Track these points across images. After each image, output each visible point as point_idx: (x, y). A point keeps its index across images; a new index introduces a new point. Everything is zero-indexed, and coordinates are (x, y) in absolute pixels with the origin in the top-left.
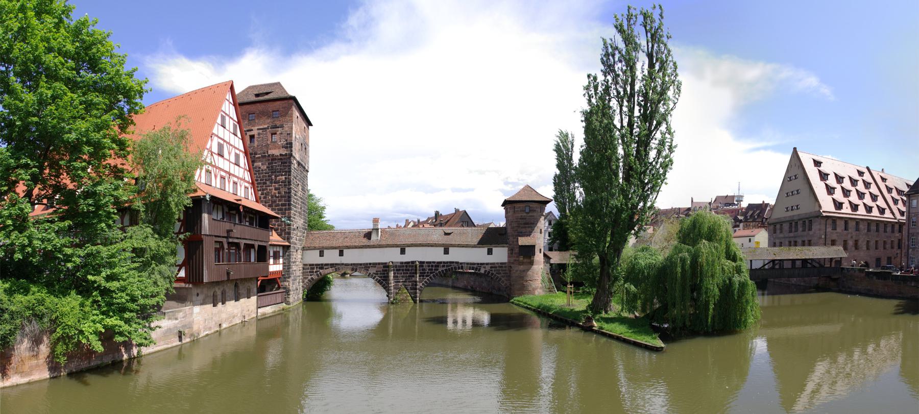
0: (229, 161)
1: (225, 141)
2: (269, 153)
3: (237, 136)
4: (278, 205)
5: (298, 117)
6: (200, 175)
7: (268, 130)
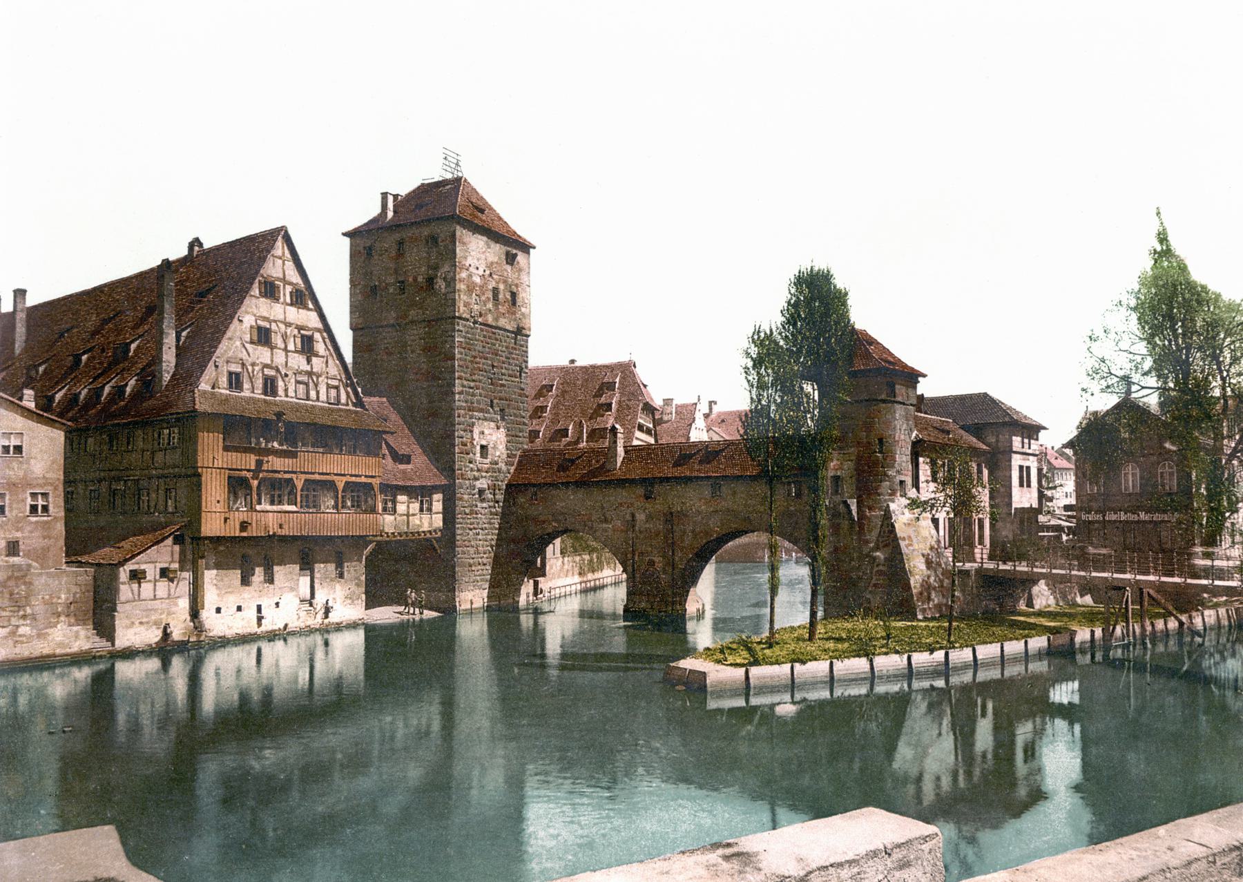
0: (286, 350)
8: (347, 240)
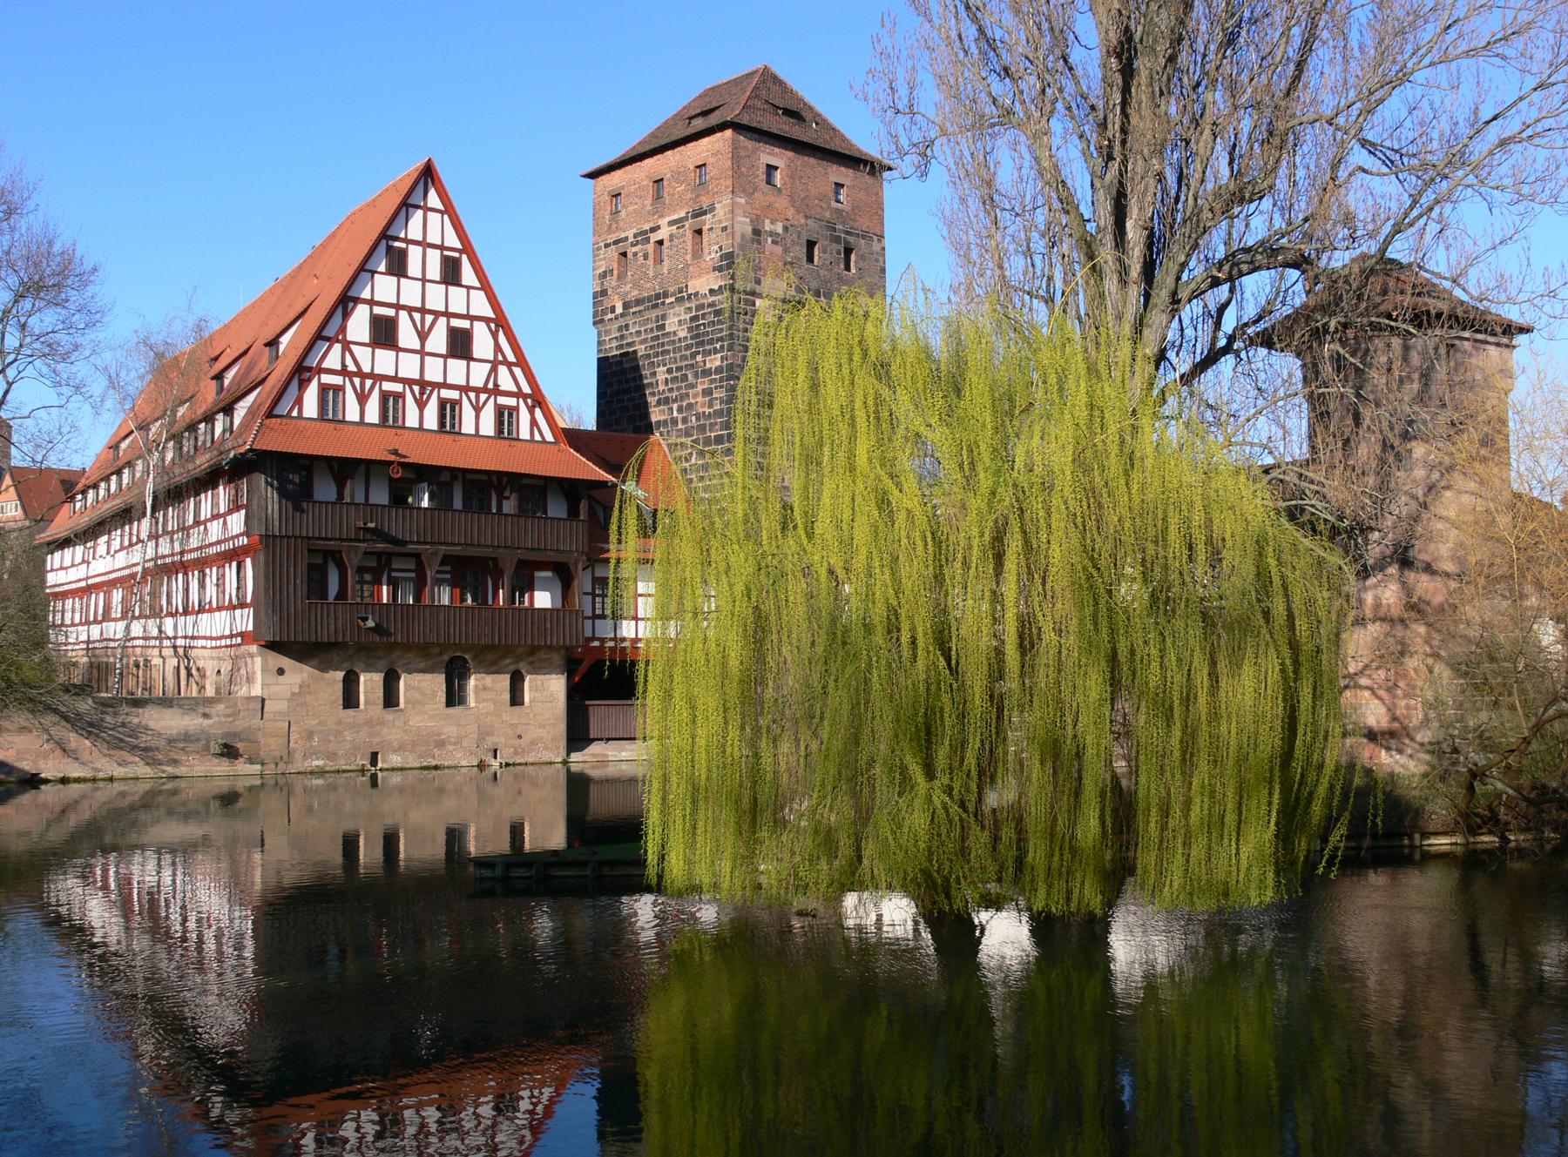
0: (422, 353)
1: (398, 307)
4: (707, 442)
6: (299, 401)
7: (687, 224)
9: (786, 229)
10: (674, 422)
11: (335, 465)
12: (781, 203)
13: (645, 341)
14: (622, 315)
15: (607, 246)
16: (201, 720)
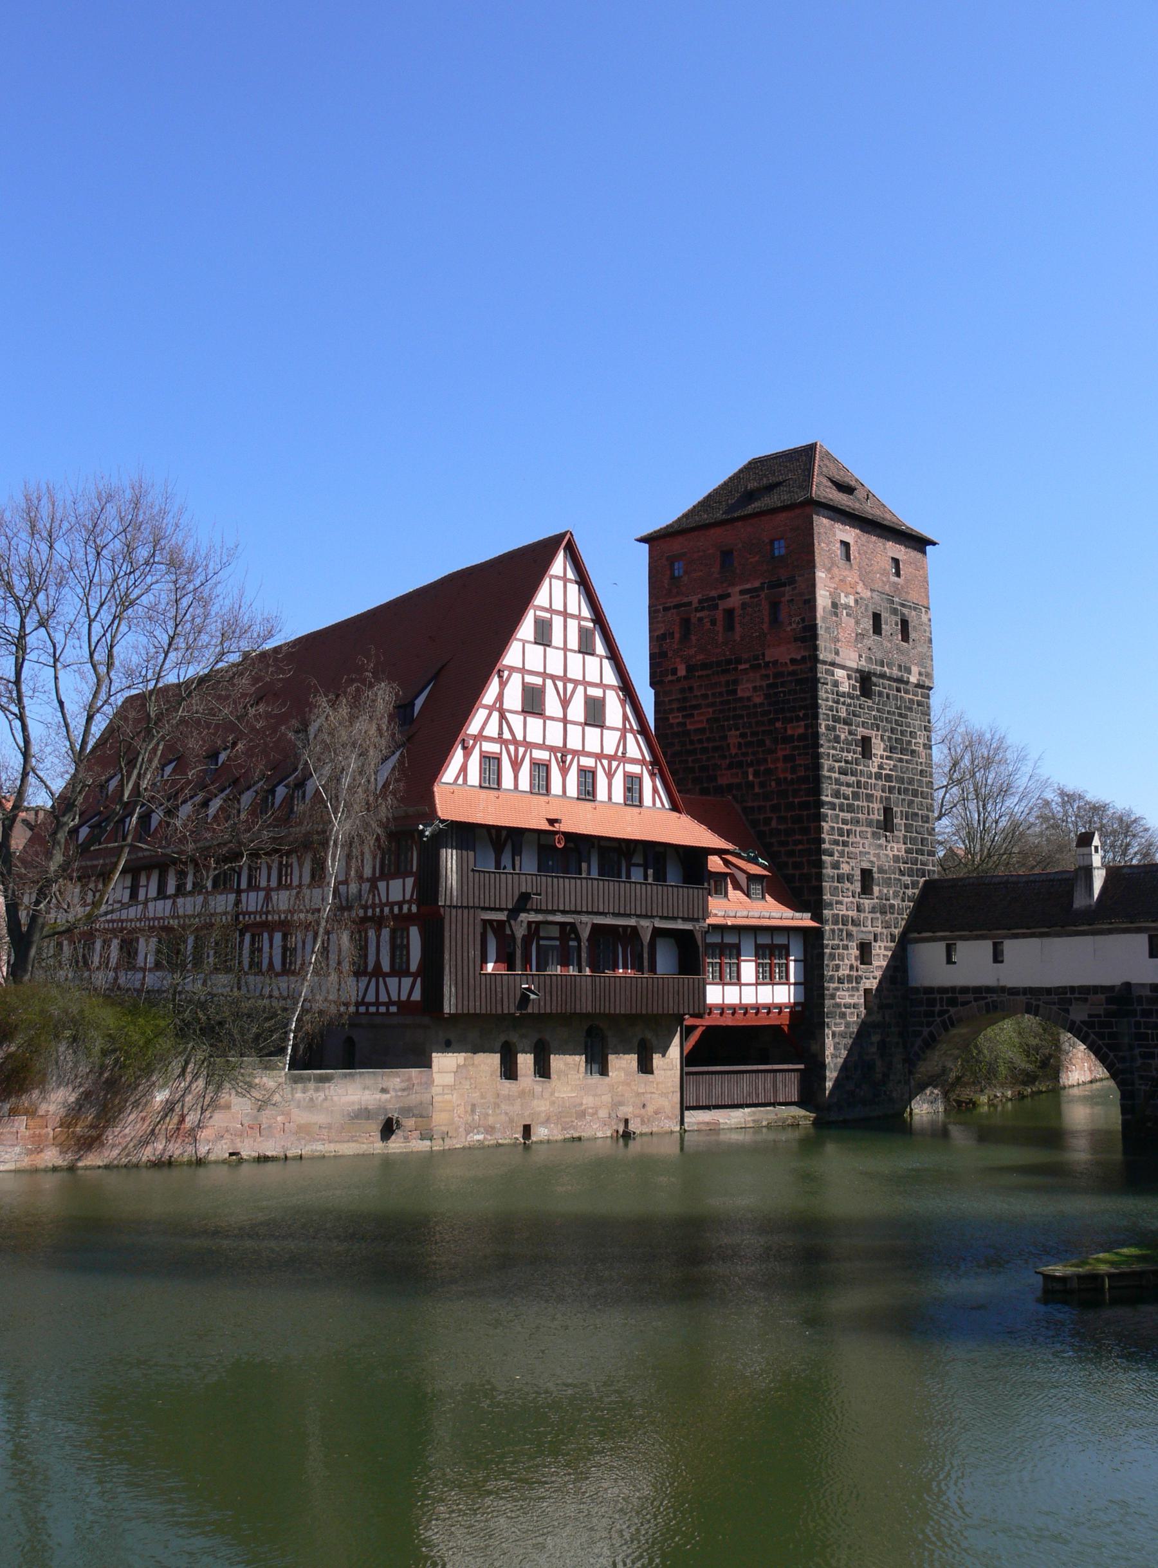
0: (565, 721)
1: (544, 675)
2: (767, 659)
3: (593, 654)
5: (846, 545)
6: (464, 769)
8: (645, 547)
9: (856, 601)
10: (751, 785)
11: (493, 832)
12: (852, 576)
13: (712, 704)
14: (685, 677)
15: (666, 609)
16: (378, 1096)
